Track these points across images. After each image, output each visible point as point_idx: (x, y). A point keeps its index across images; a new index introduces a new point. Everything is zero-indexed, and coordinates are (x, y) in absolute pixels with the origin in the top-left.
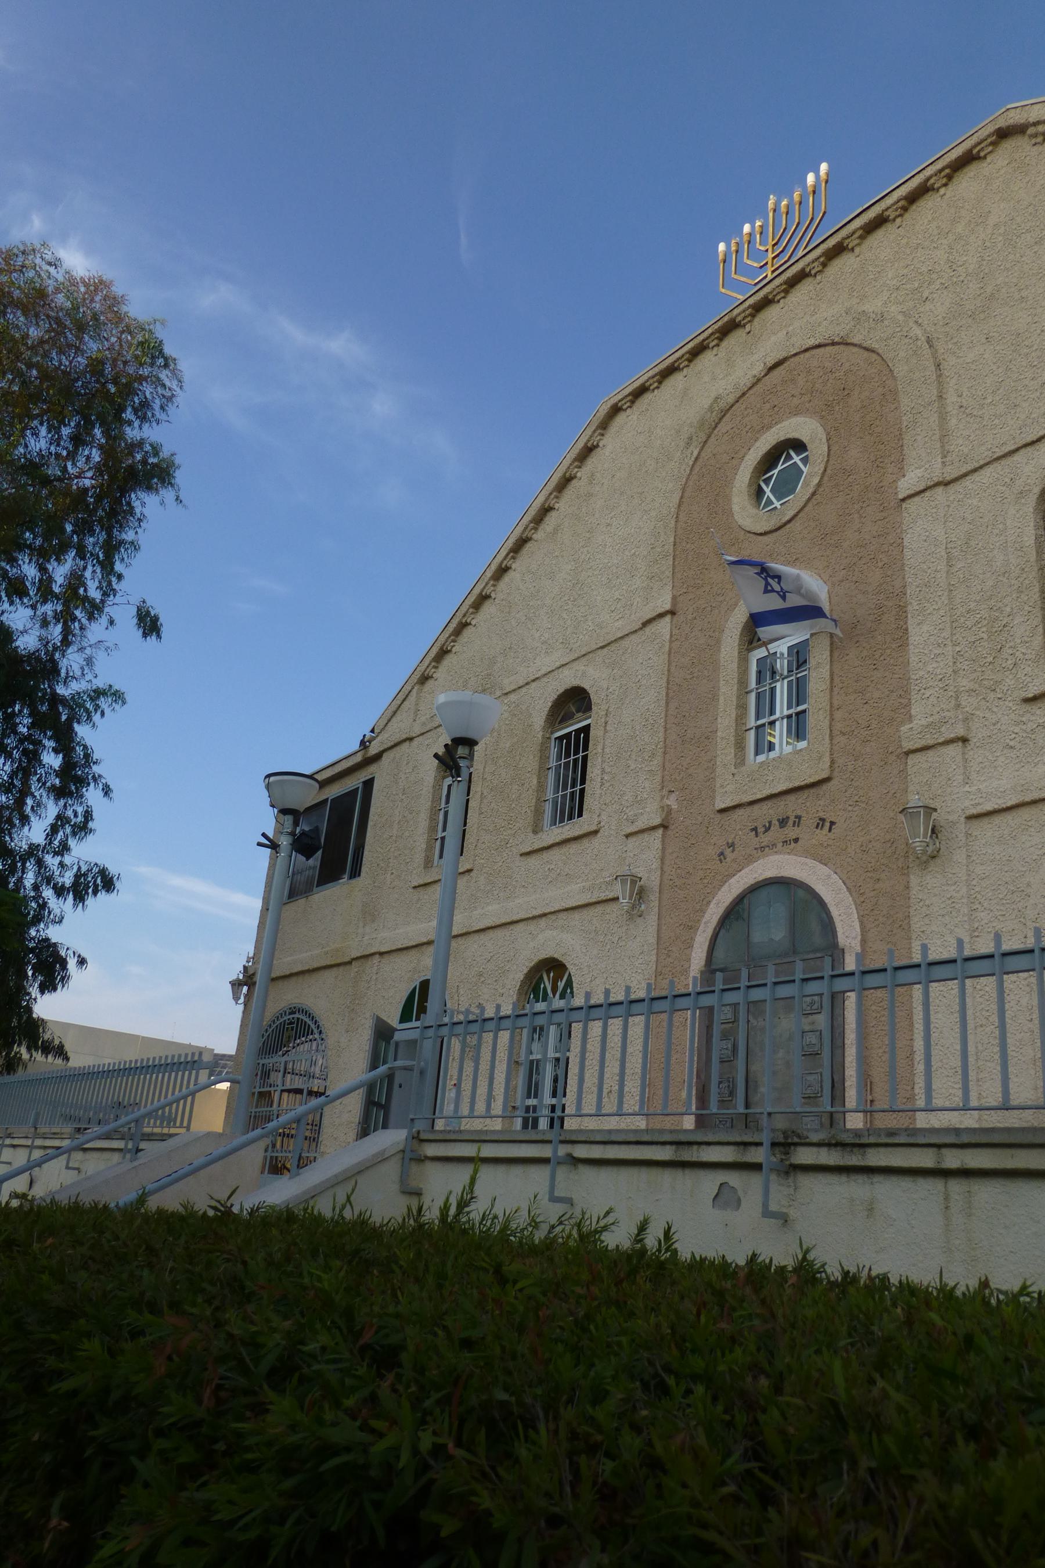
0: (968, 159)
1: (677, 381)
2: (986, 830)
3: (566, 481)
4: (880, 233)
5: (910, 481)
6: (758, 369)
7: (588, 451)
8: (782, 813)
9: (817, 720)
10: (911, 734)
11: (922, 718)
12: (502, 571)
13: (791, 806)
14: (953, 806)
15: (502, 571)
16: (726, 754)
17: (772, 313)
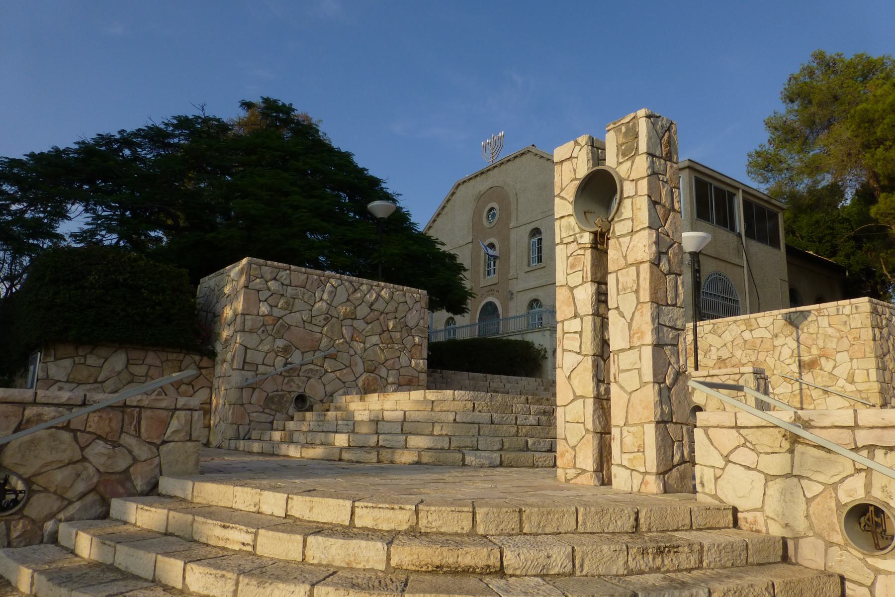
0: (523, 154)
1: (472, 181)
2: (519, 294)
3: (448, 201)
4: (510, 163)
5: (512, 225)
6: (488, 188)
7: (453, 194)
8: (491, 289)
9: (497, 271)
10: (510, 276)
11: (512, 272)
12: (434, 221)
13: (493, 287)
14: (514, 291)
15: (434, 221)
16: (482, 276)
17: (491, 172)
